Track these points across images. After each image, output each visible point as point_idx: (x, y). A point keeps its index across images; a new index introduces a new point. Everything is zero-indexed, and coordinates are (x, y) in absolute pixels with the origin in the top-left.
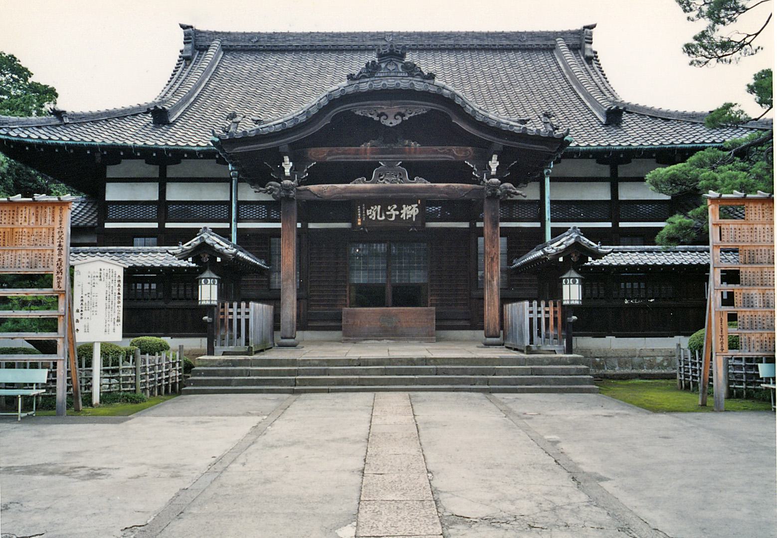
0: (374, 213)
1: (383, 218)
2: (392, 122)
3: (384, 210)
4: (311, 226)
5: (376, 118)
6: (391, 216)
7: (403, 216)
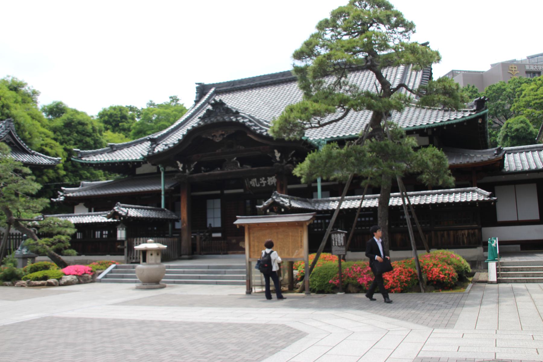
0: (253, 182)
1: (259, 185)
2: (218, 140)
3: (258, 181)
4: (226, 192)
5: (211, 138)
6: (262, 184)
7: (269, 183)
